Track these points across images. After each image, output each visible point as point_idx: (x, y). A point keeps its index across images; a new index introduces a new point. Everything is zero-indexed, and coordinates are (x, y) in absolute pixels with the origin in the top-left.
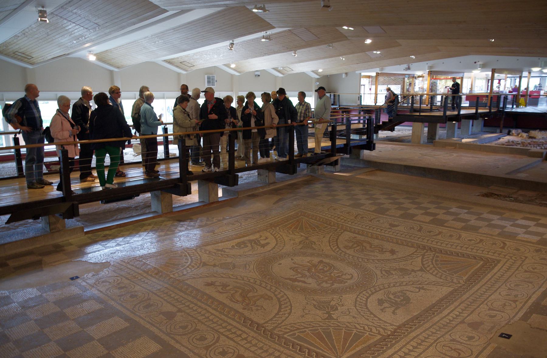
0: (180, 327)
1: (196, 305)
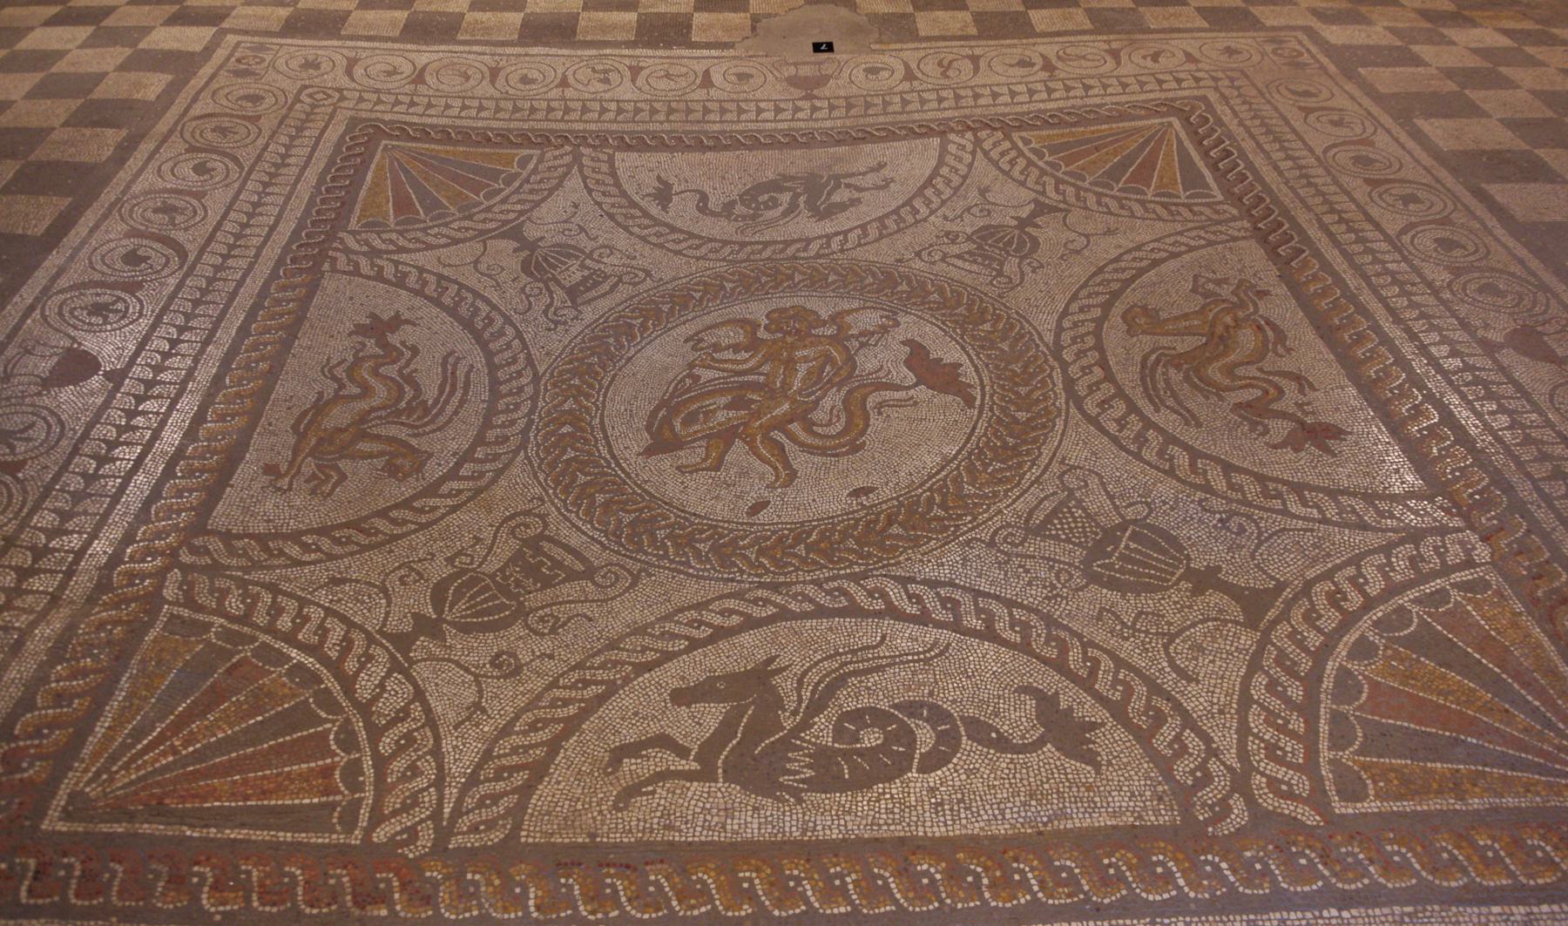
1: (1423, 349)
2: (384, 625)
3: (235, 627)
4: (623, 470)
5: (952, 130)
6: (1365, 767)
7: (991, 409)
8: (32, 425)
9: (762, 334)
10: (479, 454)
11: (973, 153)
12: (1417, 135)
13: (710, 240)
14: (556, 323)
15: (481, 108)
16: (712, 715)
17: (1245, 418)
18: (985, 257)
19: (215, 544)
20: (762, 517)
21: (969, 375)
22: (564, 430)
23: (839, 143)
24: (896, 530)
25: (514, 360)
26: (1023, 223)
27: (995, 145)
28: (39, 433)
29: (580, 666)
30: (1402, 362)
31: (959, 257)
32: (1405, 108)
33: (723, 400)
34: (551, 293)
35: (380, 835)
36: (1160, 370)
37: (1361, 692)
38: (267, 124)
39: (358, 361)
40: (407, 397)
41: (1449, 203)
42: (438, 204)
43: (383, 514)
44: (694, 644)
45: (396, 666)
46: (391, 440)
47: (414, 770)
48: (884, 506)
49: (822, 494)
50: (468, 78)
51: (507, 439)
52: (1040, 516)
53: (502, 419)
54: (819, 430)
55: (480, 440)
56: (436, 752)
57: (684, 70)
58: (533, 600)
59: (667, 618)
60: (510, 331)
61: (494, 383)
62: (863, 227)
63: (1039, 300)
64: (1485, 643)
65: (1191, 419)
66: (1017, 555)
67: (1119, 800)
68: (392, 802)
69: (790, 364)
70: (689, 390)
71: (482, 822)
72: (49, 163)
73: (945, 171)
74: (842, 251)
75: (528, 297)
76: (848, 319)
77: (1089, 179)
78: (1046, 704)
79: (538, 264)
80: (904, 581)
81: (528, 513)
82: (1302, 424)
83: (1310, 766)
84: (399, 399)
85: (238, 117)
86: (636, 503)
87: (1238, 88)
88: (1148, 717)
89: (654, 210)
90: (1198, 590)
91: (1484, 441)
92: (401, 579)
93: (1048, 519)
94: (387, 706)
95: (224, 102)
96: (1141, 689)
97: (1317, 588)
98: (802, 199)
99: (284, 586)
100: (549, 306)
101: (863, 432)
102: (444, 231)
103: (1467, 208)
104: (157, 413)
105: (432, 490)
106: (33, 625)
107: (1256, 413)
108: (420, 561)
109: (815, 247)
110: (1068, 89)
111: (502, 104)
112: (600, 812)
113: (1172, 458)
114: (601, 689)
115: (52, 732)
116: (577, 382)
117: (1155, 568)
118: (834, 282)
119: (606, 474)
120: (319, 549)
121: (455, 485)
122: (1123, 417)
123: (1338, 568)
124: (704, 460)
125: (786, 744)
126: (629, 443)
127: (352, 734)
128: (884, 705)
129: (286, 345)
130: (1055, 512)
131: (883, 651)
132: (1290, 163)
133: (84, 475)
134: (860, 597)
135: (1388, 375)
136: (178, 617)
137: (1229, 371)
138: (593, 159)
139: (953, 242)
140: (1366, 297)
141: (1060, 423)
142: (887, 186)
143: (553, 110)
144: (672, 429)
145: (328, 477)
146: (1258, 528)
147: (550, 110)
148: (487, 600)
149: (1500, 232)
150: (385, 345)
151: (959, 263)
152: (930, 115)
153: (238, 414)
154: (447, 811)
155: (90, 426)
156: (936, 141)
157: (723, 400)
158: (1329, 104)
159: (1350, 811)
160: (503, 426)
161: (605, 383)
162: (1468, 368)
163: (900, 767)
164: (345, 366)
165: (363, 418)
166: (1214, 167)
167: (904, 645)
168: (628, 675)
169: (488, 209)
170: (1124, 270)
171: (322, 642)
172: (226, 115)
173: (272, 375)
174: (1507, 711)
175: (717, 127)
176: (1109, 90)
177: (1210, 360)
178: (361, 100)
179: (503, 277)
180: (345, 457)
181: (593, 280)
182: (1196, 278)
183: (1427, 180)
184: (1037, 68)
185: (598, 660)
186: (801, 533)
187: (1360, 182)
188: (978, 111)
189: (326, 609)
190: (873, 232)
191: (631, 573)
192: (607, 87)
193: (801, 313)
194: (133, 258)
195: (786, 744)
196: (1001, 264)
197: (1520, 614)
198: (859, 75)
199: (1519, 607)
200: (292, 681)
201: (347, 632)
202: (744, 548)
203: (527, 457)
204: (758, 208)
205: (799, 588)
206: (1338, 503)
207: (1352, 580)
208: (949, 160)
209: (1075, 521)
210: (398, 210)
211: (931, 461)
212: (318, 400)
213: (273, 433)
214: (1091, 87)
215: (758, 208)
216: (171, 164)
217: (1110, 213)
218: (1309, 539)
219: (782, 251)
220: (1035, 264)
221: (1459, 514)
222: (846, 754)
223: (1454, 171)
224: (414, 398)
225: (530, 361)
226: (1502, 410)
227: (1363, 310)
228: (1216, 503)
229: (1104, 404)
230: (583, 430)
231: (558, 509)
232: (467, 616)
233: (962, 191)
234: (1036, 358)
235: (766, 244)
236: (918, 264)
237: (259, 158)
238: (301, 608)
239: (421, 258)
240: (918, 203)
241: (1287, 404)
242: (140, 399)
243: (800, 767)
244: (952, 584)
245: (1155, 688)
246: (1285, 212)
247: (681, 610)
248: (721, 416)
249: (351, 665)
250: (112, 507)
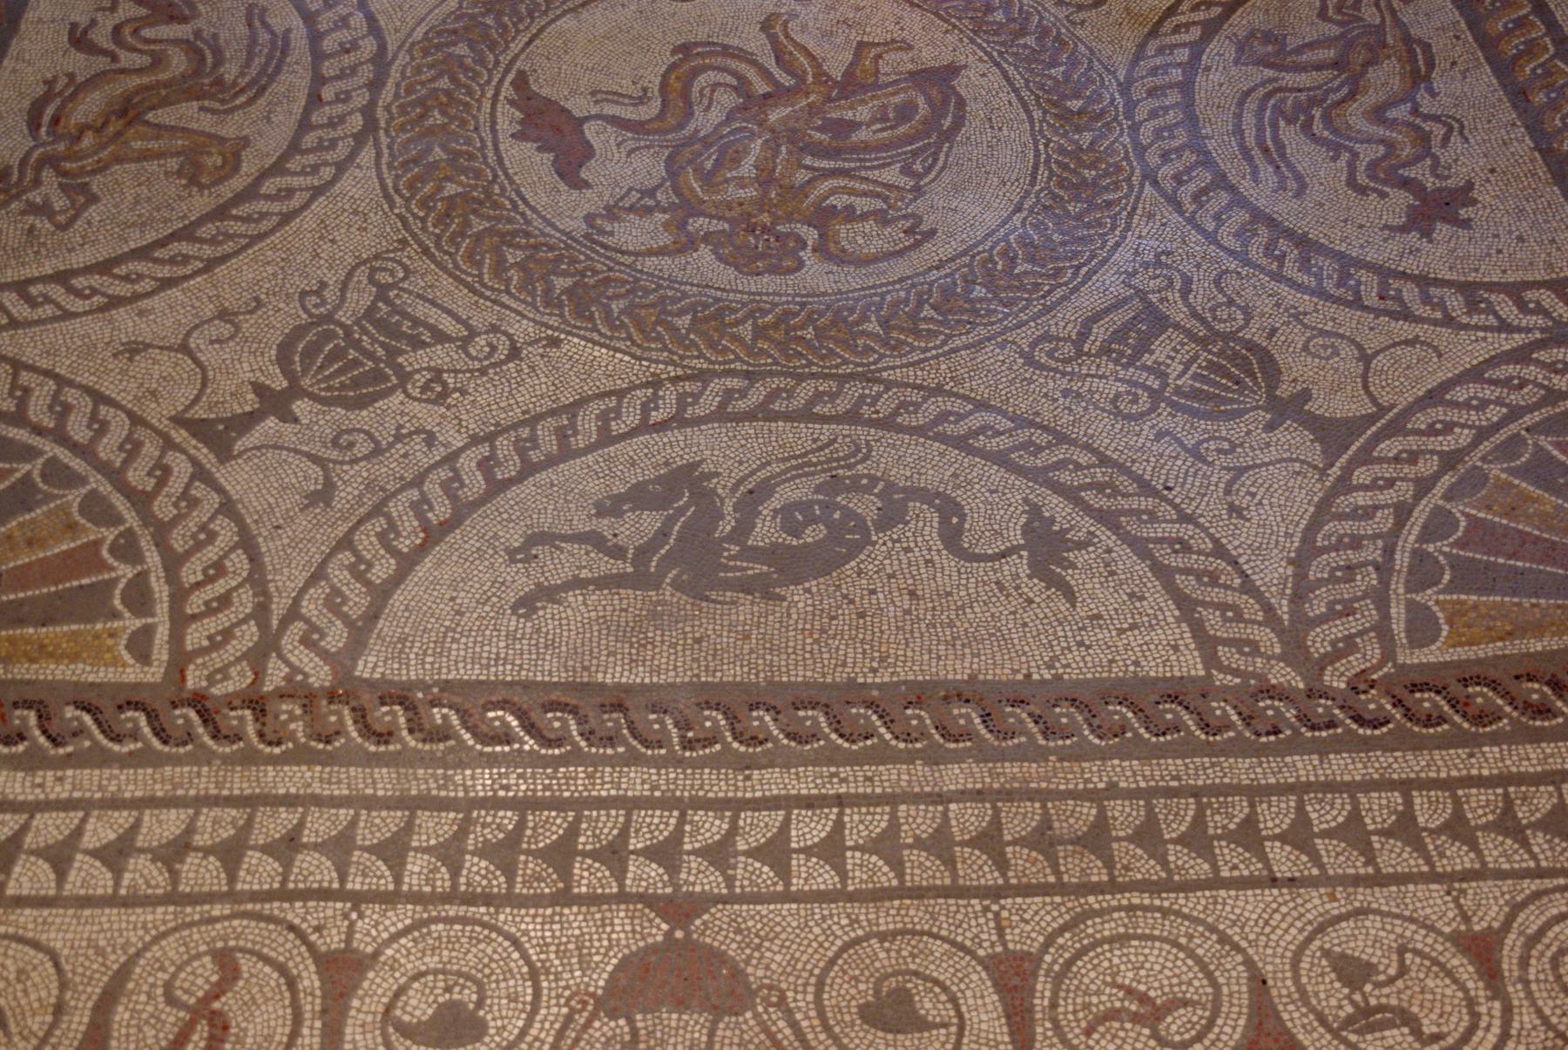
7: (497, 63)
9: (811, 235)
11: (293, 614)
18: (394, 332)
21: (508, 118)
22: (1075, 104)
23: (618, 700)
31: (441, 337)
33: (862, 135)
34: (1194, 314)
36: (242, 82)
46: (1298, 68)
60: (1230, 242)
62: (606, 438)
63: (345, 225)
69: (765, 177)
70: (915, 154)
74: (656, 383)
75: (1231, 302)
76: (665, 239)
89: (1056, 507)
98: (726, 526)
100: (1185, 292)
101: (673, 67)
116: (1089, 174)
118: (681, 313)
119: (1003, 44)
124: (879, 56)
126: (980, 82)
138: (1254, 645)
139: (438, 373)
141: (419, 34)
144: (929, 101)
151: (447, 325)
157: (862, 135)
160: (1166, 109)
164: (1436, 142)
175: (954, 776)
180: (1336, 38)
190: (588, 423)
192: (1334, 939)
193: (743, 261)
196: (372, 309)
204: (828, 507)
208: (357, 601)
215: (828, 507)
219: (773, 395)
225: (1178, 207)
230: (1055, 104)
231: (1045, 9)
233: (369, 501)
234: (402, 128)
235: (806, 415)
236: (522, 329)
240: (475, 483)
248: (863, 113)
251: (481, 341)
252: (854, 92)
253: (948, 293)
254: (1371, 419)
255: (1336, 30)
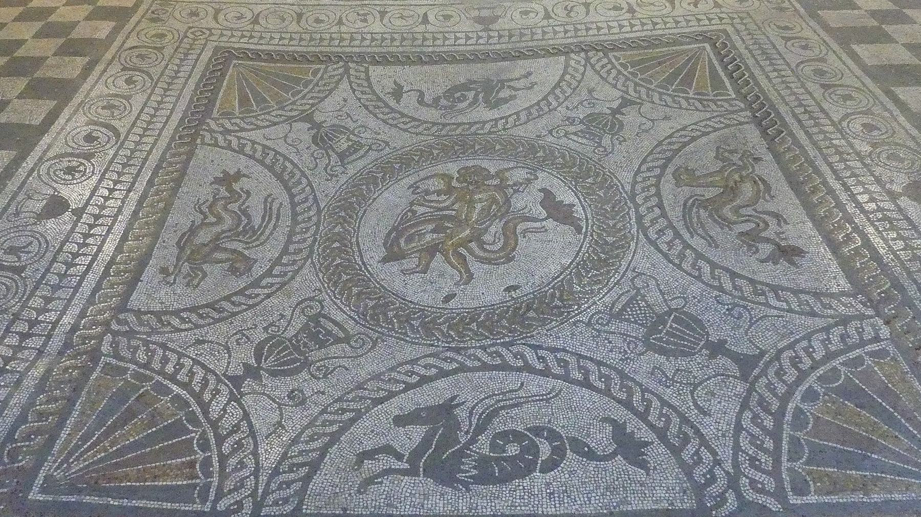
0: (902, 160)
1: (853, 197)
2: (227, 371)
3: (142, 371)
4: (369, 271)
5: (573, 51)
6: (810, 473)
8: (31, 243)
9: (455, 183)
10: (285, 260)
11: (585, 66)
12: (854, 56)
13: (426, 122)
14: (332, 176)
15: (291, 39)
16: (417, 432)
17: (744, 242)
19: (131, 318)
20: (452, 304)
22: (334, 245)
23: (504, 59)
24: (531, 314)
25: (306, 199)
26: (615, 112)
27: (598, 61)
28: (34, 248)
29: (340, 399)
30: (840, 205)
32: (846, 37)
33: (430, 227)
34: (329, 156)
35: (221, 506)
36: (695, 210)
37: (808, 424)
38: (168, 51)
39: (215, 200)
40: (243, 224)
41: (871, 100)
42: (265, 101)
43: (227, 298)
44: (409, 387)
45: (232, 398)
47: (242, 465)
48: (525, 298)
49: (488, 289)
50: (283, 20)
51: (301, 250)
52: (619, 306)
53: (299, 237)
54: (488, 247)
55: (285, 251)
56: (255, 454)
57: (412, 13)
58: (315, 355)
59: (392, 369)
60: (304, 181)
61: (295, 215)
62: (517, 114)
63: (623, 162)
64: (885, 392)
65: (712, 242)
66: (605, 332)
67: (660, 493)
68: (229, 484)
69: (471, 203)
70: (410, 220)
71: (280, 499)
72: (45, 79)
73: (568, 77)
74: (504, 129)
75: (315, 159)
76: (507, 174)
77: (655, 83)
78: (619, 428)
79: (322, 139)
80: (535, 348)
81: (311, 299)
82: (778, 245)
83: (775, 473)
84: (238, 225)
85: (151, 48)
86: (376, 293)
87: (745, 25)
88: (679, 437)
89: (392, 103)
90: (712, 356)
91: (888, 258)
92: (237, 341)
93: (624, 309)
94: (227, 424)
95: (144, 39)
96: (676, 420)
97: (786, 354)
98: (481, 95)
99: (170, 345)
100: (327, 165)
101: (514, 249)
102: (267, 117)
103: (882, 103)
104: (101, 235)
105: (256, 284)
106: (28, 369)
107: (751, 239)
108: (248, 329)
109: (488, 126)
110: (643, 24)
111: (303, 36)
112: (350, 494)
113: (699, 269)
114: (352, 415)
115: (36, 437)
117: (688, 341)
118: (499, 150)
120: (190, 321)
121: (270, 280)
122: (671, 241)
123: (797, 341)
124: (418, 266)
125: (460, 454)
126: (373, 254)
127: (207, 440)
128: (520, 428)
129: (175, 191)
130: (627, 304)
131: (522, 393)
132: (776, 74)
133: (58, 274)
134: (509, 358)
135: (831, 213)
136: (109, 364)
137: (736, 210)
139: (571, 124)
140: (819, 162)
141: (633, 245)
142: (531, 88)
143: (333, 39)
145: (197, 275)
146: (751, 315)
147: (332, 39)
148: (285, 356)
149: (902, 119)
150: (230, 190)
151: (575, 138)
152: (558, 42)
153: (146, 235)
154: (260, 491)
155: (63, 244)
156: (563, 58)
157: (430, 227)
158: (799, 35)
159: (799, 502)
161: (360, 214)
162: (880, 210)
163: (529, 469)
164: (208, 204)
165: (217, 237)
166: (731, 77)
167: (534, 390)
168: (368, 406)
169: (294, 103)
170: (674, 143)
171: (191, 381)
172: (145, 47)
173: (166, 210)
174: (896, 437)
175: (430, 49)
176: (668, 25)
177: (725, 204)
178: (222, 35)
179: (301, 147)
181: (355, 148)
182: (718, 148)
183: (858, 85)
184: (624, 11)
185: (350, 396)
186: (473, 315)
187: (818, 86)
188: (589, 39)
189: (193, 359)
190: (523, 117)
191: (372, 340)
193: (479, 170)
194: (89, 138)
195: (460, 454)
196: (601, 139)
197: (907, 372)
198: (517, 16)
199: (906, 368)
200: (173, 405)
201: (206, 374)
202: (440, 324)
203: (312, 263)
205: (472, 351)
206: (799, 298)
207: (805, 350)
208: (570, 70)
209: (640, 310)
210: (241, 105)
211: (554, 269)
212: (192, 225)
213: (165, 247)
214: (657, 24)
216: (113, 78)
217: (667, 105)
218: (779, 323)
220: (621, 139)
221: (871, 307)
222: (497, 460)
223: (874, 78)
224: (248, 223)
226: (900, 237)
227: (817, 171)
228: (725, 298)
229: (661, 232)
232: (275, 365)
235: (459, 125)
236: (550, 139)
237: (162, 74)
238: (179, 359)
239: (256, 135)
240: (551, 99)
241: (769, 233)
242: (91, 227)
243: (469, 468)
244: (564, 350)
245: (685, 420)
246: (772, 106)
247: (401, 364)
248: (428, 237)
249: (207, 396)
250: (74, 294)
251: (562, 134)
252: (431, 247)
253: (408, 165)
254: (295, 121)
255: (205, 267)
